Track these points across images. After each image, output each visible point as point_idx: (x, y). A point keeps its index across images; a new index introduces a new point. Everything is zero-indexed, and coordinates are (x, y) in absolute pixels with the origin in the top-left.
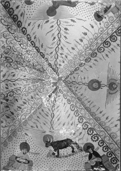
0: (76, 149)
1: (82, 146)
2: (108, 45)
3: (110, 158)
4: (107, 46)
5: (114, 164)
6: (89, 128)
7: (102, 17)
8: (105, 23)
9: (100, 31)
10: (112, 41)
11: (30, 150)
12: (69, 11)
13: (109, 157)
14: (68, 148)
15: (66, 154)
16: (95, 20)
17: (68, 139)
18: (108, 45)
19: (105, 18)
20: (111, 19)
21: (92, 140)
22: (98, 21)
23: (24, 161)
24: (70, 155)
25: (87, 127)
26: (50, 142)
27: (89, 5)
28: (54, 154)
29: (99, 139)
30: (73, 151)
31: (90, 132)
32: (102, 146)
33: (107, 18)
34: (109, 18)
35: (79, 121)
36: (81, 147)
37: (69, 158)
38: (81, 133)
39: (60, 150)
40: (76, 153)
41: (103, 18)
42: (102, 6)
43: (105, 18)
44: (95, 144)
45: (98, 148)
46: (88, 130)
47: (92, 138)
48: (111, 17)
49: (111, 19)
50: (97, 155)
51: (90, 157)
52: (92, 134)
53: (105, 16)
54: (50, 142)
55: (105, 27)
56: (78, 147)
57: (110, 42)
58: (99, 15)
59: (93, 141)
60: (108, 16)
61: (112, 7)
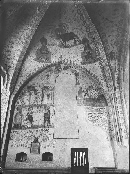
0: (77, 42)
1: (81, 39)
3: (97, 52)
5: (98, 56)
6: (88, 26)
11: (48, 43)
13: (97, 51)
14: (72, 40)
15: (70, 45)
17: (72, 33)
21: (88, 36)
23: (46, 52)
24: (73, 46)
25: (86, 26)
26: (59, 34)
28: (63, 44)
29: (92, 36)
30: (75, 43)
31: (88, 30)
32: (94, 42)
35: (80, 19)
36: (80, 40)
37: (72, 48)
38: (81, 29)
39: (67, 42)
40: (77, 45)
44: (90, 39)
45: (91, 43)
46: (87, 28)
47: (88, 35)
50: (89, 48)
51: (85, 50)
52: (89, 31)
54: (59, 34)
56: (79, 40)
59: (89, 37)
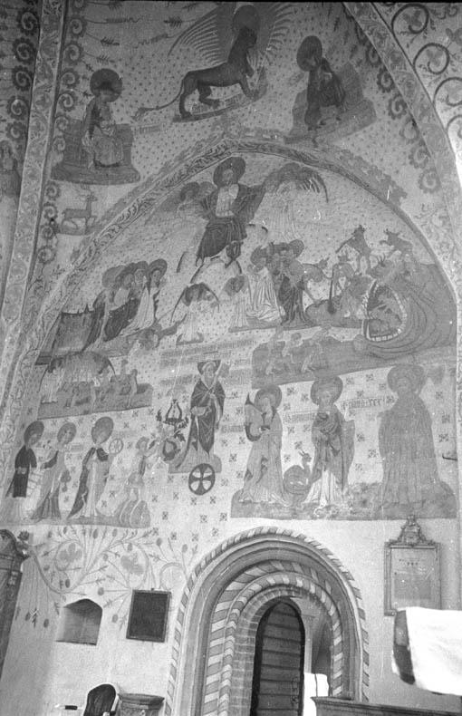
2: (26, 21)
4: (25, 16)
7: (97, 91)
8: (77, 82)
9: (75, 49)
10: (22, 40)
12: (197, 51)
16: (110, 66)
18: (26, 21)
19: (85, 94)
20: (68, 103)
22: (99, 72)
27: (147, 106)
33: (80, 97)
34: (75, 99)
41: (92, 89)
42: (111, 122)
43: (85, 94)
48: (73, 108)
49: (68, 103)
53: (90, 99)
55: (71, 71)
57: (28, 40)
58: (108, 91)
60: (82, 103)
61: (87, 136)
